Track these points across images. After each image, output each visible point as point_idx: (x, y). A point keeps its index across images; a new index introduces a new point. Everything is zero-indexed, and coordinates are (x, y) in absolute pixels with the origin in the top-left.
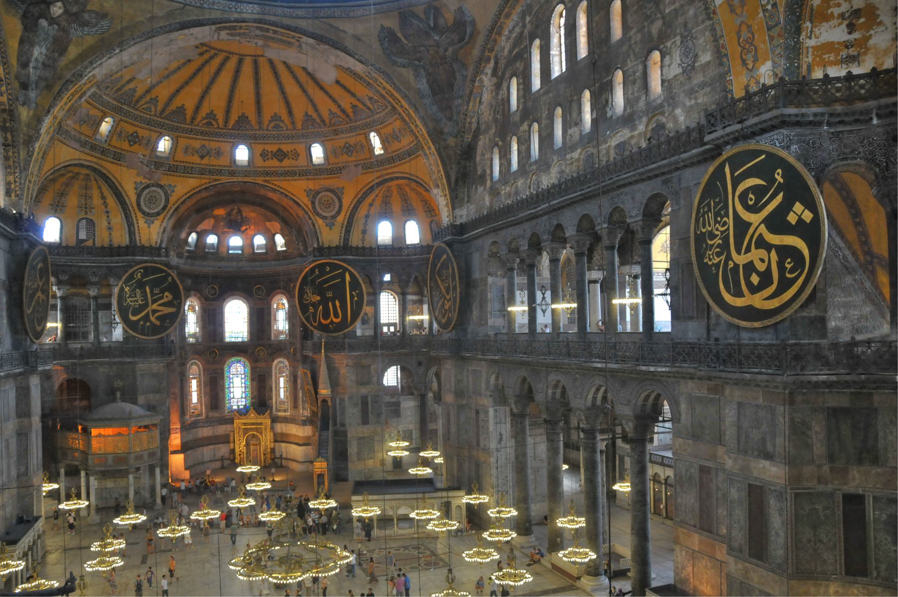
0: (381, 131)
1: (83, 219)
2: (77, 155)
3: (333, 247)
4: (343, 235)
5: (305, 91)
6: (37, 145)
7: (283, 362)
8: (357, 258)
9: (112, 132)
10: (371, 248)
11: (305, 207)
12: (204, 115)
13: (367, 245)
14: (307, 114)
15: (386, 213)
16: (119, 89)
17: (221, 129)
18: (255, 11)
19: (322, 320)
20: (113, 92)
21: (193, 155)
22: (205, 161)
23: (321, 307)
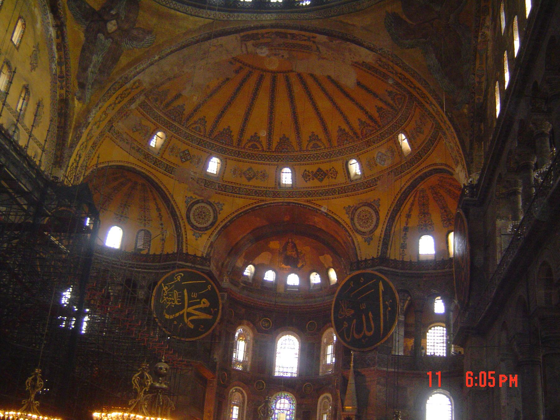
0: (407, 129)
1: (142, 230)
2: (131, 159)
3: (369, 260)
4: (380, 248)
5: (334, 103)
6: (85, 132)
7: (327, 398)
8: (394, 270)
9: (166, 145)
10: (411, 262)
11: (345, 226)
12: (249, 138)
13: (406, 259)
14: (340, 130)
15: (426, 225)
16: (168, 105)
17: (266, 151)
18: (272, 18)
19: (356, 336)
20: (162, 106)
21: (241, 177)
22: (251, 183)
23: (355, 321)
